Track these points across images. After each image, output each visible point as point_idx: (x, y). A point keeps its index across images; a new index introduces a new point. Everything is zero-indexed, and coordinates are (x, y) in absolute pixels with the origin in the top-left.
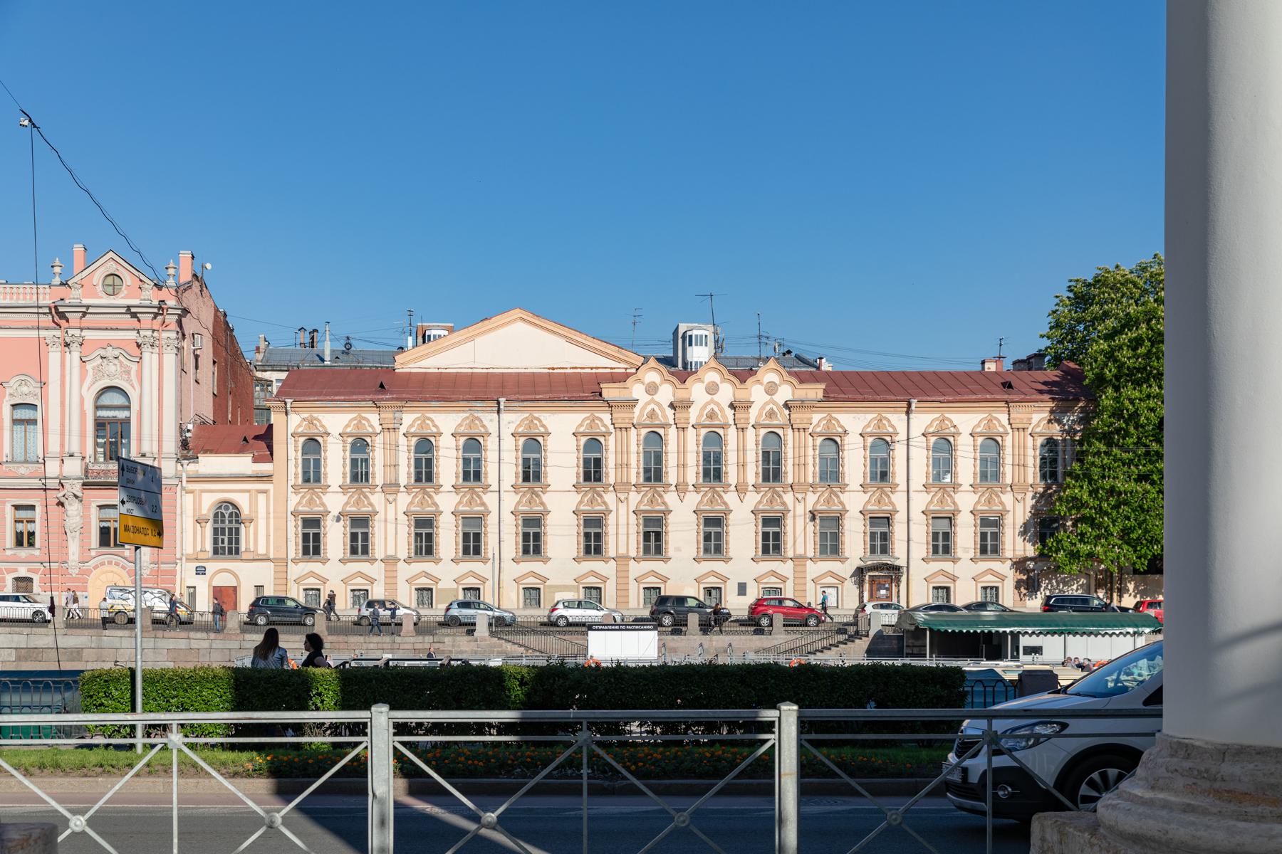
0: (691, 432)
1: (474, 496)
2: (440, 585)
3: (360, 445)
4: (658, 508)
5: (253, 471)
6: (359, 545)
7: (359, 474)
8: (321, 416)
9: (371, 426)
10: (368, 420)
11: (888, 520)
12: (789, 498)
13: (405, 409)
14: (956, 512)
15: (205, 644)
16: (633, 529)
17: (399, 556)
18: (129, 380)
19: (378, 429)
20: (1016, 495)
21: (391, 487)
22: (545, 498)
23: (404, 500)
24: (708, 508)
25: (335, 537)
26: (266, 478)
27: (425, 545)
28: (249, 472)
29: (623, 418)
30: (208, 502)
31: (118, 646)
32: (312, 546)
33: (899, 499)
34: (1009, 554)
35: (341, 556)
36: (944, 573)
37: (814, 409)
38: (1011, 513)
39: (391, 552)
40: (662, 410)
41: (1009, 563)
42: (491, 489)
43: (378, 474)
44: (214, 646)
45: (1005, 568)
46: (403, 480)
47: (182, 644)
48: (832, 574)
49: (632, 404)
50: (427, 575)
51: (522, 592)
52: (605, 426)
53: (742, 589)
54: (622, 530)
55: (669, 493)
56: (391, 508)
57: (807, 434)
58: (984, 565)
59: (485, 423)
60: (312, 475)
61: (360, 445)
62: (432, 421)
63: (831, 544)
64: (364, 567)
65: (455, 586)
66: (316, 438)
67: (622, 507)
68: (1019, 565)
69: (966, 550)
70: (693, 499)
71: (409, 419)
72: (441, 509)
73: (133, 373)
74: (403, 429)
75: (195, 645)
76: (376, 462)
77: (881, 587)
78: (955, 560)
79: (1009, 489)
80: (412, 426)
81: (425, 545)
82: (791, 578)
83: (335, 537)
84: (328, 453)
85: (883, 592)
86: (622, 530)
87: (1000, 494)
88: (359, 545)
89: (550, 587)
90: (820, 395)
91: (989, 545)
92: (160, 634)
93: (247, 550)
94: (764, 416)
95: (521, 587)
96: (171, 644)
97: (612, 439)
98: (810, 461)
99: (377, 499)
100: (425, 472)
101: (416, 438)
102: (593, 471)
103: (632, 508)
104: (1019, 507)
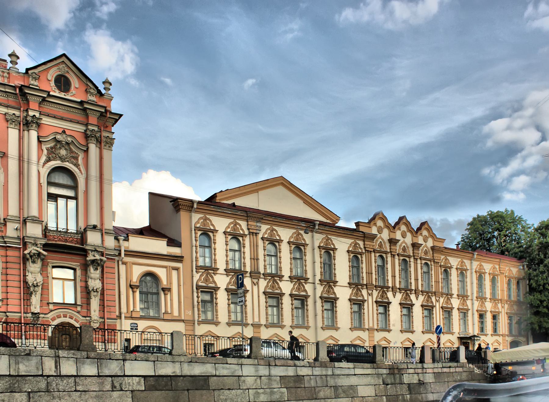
1: (209, 276)
5: (168, 252)
10: (240, 226)
14: (452, 308)
17: (249, 322)
18: (77, 165)
19: (246, 232)
26: (178, 259)
28: (165, 253)
29: (370, 246)
30: (137, 271)
33: (469, 303)
49: (373, 237)
55: (217, 275)
62: (276, 231)
73: (80, 161)
74: (260, 236)
80: (265, 233)
93: (166, 312)
97: (364, 256)
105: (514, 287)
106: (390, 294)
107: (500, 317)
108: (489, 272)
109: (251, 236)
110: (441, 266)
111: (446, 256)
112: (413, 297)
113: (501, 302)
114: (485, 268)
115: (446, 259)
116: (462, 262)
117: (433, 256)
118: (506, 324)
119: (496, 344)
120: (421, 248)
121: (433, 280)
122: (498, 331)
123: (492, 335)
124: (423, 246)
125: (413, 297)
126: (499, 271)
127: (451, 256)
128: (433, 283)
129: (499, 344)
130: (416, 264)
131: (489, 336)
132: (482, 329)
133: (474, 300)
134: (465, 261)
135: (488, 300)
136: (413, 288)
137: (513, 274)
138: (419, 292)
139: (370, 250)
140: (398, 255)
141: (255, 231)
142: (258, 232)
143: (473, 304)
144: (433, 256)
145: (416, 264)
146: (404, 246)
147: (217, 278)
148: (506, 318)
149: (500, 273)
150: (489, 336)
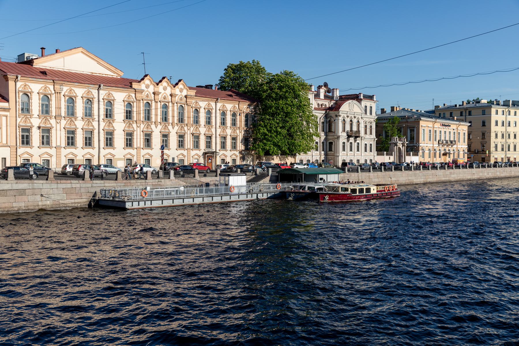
0: (159, 104)
2: (77, 158)
3: (46, 98)
4: (149, 130)
6: (46, 141)
7: (46, 110)
8: (29, 84)
9: (51, 91)
10: (49, 88)
11: (92, 132)
13: (64, 85)
15: (78, 186)
16: (142, 137)
20: (57, 121)
21: (58, 117)
22: (114, 124)
23: (63, 122)
24: (23, 124)
25: (36, 136)
27: (71, 142)
31: (42, 187)
32: (26, 141)
33: (213, 130)
34: (238, 149)
35: (39, 145)
38: (55, 128)
39: (58, 144)
40: (150, 95)
41: (238, 152)
42: (95, 120)
43: (53, 111)
44: (81, 186)
45: (237, 153)
46: (63, 114)
47: (69, 186)
48: (197, 155)
49: (142, 91)
50: (73, 154)
51: (67, 160)
52: (133, 99)
53: (173, 159)
54: (139, 137)
56: (58, 125)
58: (233, 152)
59: (93, 93)
60: (26, 109)
61: (46, 98)
63: (197, 145)
64: (48, 150)
65: (83, 158)
66: (28, 94)
67: (138, 129)
68: (241, 153)
71: (65, 89)
72: (77, 127)
74: (62, 94)
75: (74, 186)
76: (52, 106)
77: (209, 159)
81: (71, 142)
82: (186, 155)
83: (36, 136)
84: (77, 104)
85: (210, 161)
86: (139, 137)
88: (46, 141)
89: (116, 158)
90: (194, 94)
91: (234, 147)
92: (59, 181)
95: (67, 159)
96: (64, 186)
98: (191, 116)
99: (53, 121)
100: (71, 113)
101: (86, 99)
102: (129, 115)
103: (142, 130)
104: (240, 134)
106: (153, 126)
109: (57, 94)
112: (170, 127)
117: (186, 102)
121: (186, 116)
125: (170, 127)
130: (173, 106)
134: (211, 103)
135: (229, 128)
139: (139, 99)
141: (59, 91)
142: (61, 91)
143: (216, 131)
144: (186, 102)
145: (173, 106)
147: (32, 120)
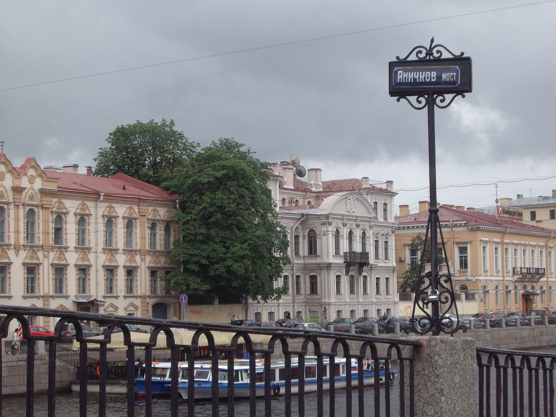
12: (40, 254)
36: (113, 306)
37: (55, 196)
57: (49, 211)
69: (121, 291)
70: (23, 255)
78: (117, 297)
79: (138, 253)
87: (134, 255)
94: (28, 198)
105: (160, 232)
107: (41, 271)
108: (123, 215)
110: (52, 212)
111: (59, 199)
113: (140, 253)
114: (117, 209)
115: (61, 203)
116: (84, 204)
118: (51, 280)
119: (131, 308)
120: (24, 192)
122: (134, 291)
123: (125, 297)
124: (26, 190)
126: (138, 214)
127: (67, 198)
128: (41, 236)
129: (136, 308)
131: (121, 299)
132: (110, 288)
133: (98, 253)
136: (12, 242)
137: (159, 215)
138: (20, 247)
140: (23, 205)
146: (32, 193)
148: (51, 272)
149: (140, 215)
150: (121, 299)
